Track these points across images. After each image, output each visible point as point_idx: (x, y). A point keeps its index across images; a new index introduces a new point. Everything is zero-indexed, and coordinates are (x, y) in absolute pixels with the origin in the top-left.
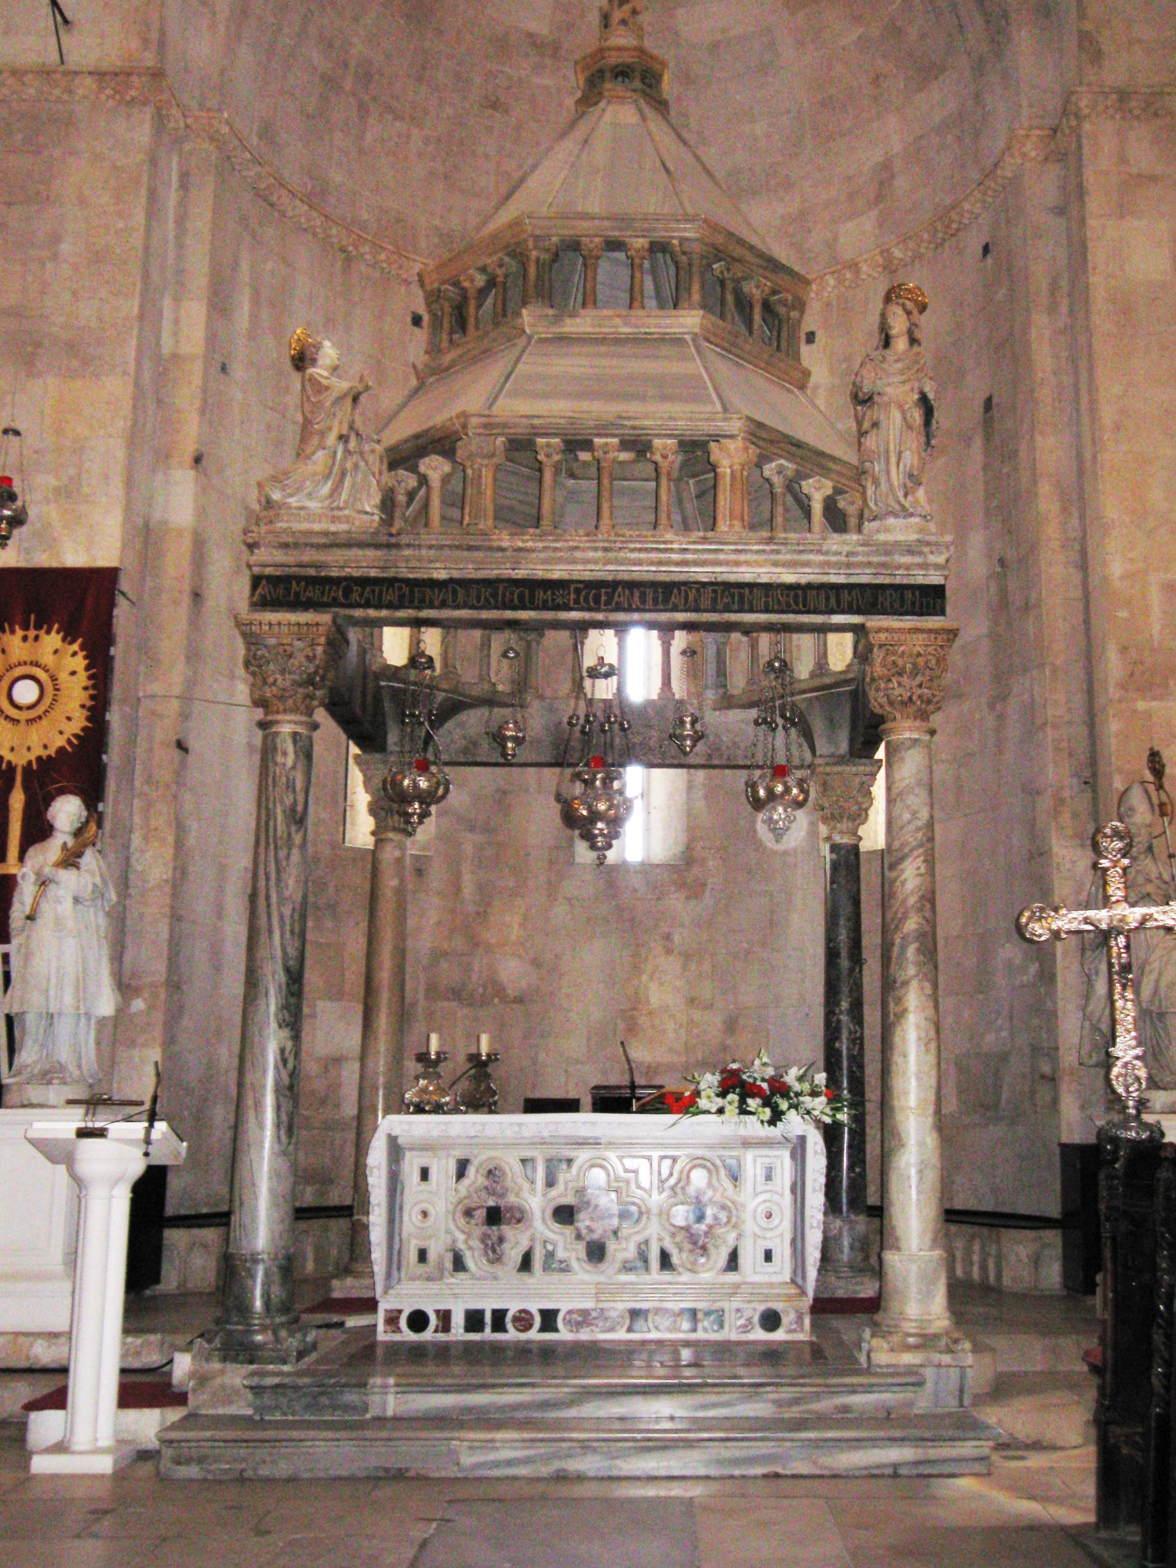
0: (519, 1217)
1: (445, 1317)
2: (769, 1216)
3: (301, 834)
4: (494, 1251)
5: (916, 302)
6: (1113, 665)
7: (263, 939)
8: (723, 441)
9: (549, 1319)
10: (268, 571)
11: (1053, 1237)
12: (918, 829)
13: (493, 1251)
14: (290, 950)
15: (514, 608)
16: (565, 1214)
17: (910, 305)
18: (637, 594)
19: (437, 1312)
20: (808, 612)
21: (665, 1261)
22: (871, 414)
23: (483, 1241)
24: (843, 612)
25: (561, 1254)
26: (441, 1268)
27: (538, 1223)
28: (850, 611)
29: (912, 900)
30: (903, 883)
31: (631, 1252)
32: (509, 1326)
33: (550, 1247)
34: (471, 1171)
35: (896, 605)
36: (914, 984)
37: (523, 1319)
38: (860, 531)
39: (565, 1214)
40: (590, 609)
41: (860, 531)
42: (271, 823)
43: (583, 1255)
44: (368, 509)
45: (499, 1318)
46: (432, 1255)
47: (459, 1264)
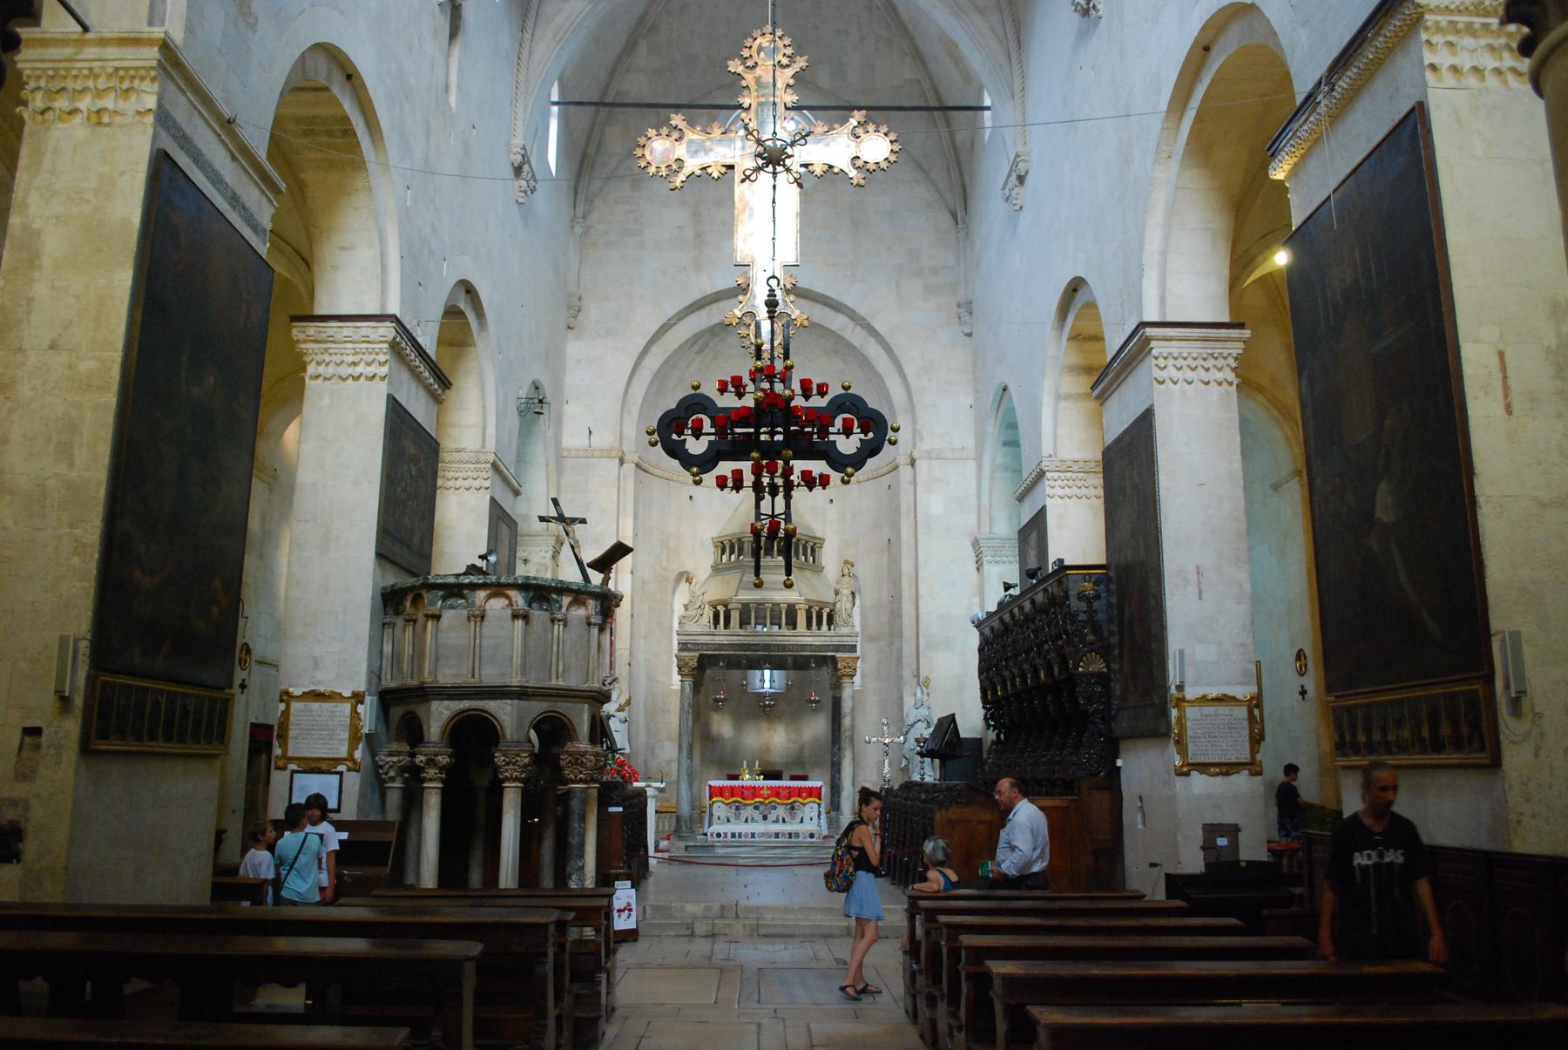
1: (726, 834)
9: (753, 835)
13: (737, 817)
17: (849, 566)
22: (839, 597)
26: (723, 820)
31: (775, 819)
36: (848, 749)
45: (740, 834)
46: (721, 818)
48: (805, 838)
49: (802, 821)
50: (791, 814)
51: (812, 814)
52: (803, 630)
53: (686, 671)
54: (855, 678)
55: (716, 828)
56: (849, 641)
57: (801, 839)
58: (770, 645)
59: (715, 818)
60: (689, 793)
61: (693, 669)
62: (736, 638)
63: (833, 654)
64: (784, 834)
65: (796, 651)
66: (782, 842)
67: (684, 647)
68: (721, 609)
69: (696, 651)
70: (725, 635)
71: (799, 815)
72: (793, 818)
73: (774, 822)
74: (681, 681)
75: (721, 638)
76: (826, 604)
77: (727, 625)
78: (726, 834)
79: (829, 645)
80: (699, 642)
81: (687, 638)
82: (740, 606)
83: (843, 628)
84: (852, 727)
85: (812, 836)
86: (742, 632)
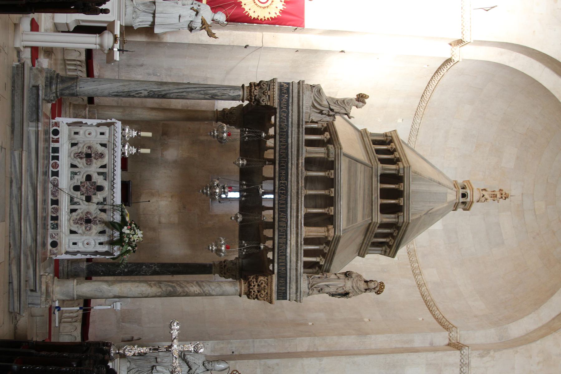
1: (57, 141)
2: (88, 244)
3: (208, 98)
4: (77, 156)
5: (378, 291)
7: (176, 87)
8: (333, 229)
9: (56, 174)
10: (291, 87)
12: (209, 291)
13: (78, 155)
14: (172, 95)
15: (279, 163)
16: (89, 178)
17: (377, 289)
18: (283, 202)
19: (58, 138)
20: (278, 256)
21: (73, 211)
22: (342, 276)
23: (80, 152)
24: (278, 267)
25: (76, 177)
26: (72, 139)
27: (86, 169)
28: (278, 270)
29: (186, 289)
30: (192, 286)
31: (76, 200)
32: (54, 161)
33: (78, 174)
34: (103, 148)
35: (280, 284)
36: (160, 290)
37: (56, 166)
38: (304, 273)
39: (89, 178)
40: (279, 187)
41: (304, 273)
42: (212, 89)
44: (311, 118)
45: (57, 158)
46: (76, 136)
47: (73, 145)
48: (52, 236)
49: (72, 232)
50: (81, 219)
51: (80, 245)
52: (303, 236)
53: (256, 92)
54: (245, 297)
57: (50, 231)
58: (286, 194)
59: (77, 129)
60: (106, 93)
61: (258, 101)
62: (295, 153)
63: (276, 271)
64: (57, 210)
65: (279, 226)
66: (44, 209)
67: (285, 89)
68: (327, 135)
69: (280, 103)
70: (298, 140)
71: (80, 229)
72: (76, 222)
74: (243, 86)
75: (295, 136)
76: (330, 261)
77: (310, 143)
78: (57, 141)
79: (286, 266)
80: (290, 108)
82: (332, 158)
83: (307, 282)
84: (187, 295)
85: (54, 244)
86: (302, 161)
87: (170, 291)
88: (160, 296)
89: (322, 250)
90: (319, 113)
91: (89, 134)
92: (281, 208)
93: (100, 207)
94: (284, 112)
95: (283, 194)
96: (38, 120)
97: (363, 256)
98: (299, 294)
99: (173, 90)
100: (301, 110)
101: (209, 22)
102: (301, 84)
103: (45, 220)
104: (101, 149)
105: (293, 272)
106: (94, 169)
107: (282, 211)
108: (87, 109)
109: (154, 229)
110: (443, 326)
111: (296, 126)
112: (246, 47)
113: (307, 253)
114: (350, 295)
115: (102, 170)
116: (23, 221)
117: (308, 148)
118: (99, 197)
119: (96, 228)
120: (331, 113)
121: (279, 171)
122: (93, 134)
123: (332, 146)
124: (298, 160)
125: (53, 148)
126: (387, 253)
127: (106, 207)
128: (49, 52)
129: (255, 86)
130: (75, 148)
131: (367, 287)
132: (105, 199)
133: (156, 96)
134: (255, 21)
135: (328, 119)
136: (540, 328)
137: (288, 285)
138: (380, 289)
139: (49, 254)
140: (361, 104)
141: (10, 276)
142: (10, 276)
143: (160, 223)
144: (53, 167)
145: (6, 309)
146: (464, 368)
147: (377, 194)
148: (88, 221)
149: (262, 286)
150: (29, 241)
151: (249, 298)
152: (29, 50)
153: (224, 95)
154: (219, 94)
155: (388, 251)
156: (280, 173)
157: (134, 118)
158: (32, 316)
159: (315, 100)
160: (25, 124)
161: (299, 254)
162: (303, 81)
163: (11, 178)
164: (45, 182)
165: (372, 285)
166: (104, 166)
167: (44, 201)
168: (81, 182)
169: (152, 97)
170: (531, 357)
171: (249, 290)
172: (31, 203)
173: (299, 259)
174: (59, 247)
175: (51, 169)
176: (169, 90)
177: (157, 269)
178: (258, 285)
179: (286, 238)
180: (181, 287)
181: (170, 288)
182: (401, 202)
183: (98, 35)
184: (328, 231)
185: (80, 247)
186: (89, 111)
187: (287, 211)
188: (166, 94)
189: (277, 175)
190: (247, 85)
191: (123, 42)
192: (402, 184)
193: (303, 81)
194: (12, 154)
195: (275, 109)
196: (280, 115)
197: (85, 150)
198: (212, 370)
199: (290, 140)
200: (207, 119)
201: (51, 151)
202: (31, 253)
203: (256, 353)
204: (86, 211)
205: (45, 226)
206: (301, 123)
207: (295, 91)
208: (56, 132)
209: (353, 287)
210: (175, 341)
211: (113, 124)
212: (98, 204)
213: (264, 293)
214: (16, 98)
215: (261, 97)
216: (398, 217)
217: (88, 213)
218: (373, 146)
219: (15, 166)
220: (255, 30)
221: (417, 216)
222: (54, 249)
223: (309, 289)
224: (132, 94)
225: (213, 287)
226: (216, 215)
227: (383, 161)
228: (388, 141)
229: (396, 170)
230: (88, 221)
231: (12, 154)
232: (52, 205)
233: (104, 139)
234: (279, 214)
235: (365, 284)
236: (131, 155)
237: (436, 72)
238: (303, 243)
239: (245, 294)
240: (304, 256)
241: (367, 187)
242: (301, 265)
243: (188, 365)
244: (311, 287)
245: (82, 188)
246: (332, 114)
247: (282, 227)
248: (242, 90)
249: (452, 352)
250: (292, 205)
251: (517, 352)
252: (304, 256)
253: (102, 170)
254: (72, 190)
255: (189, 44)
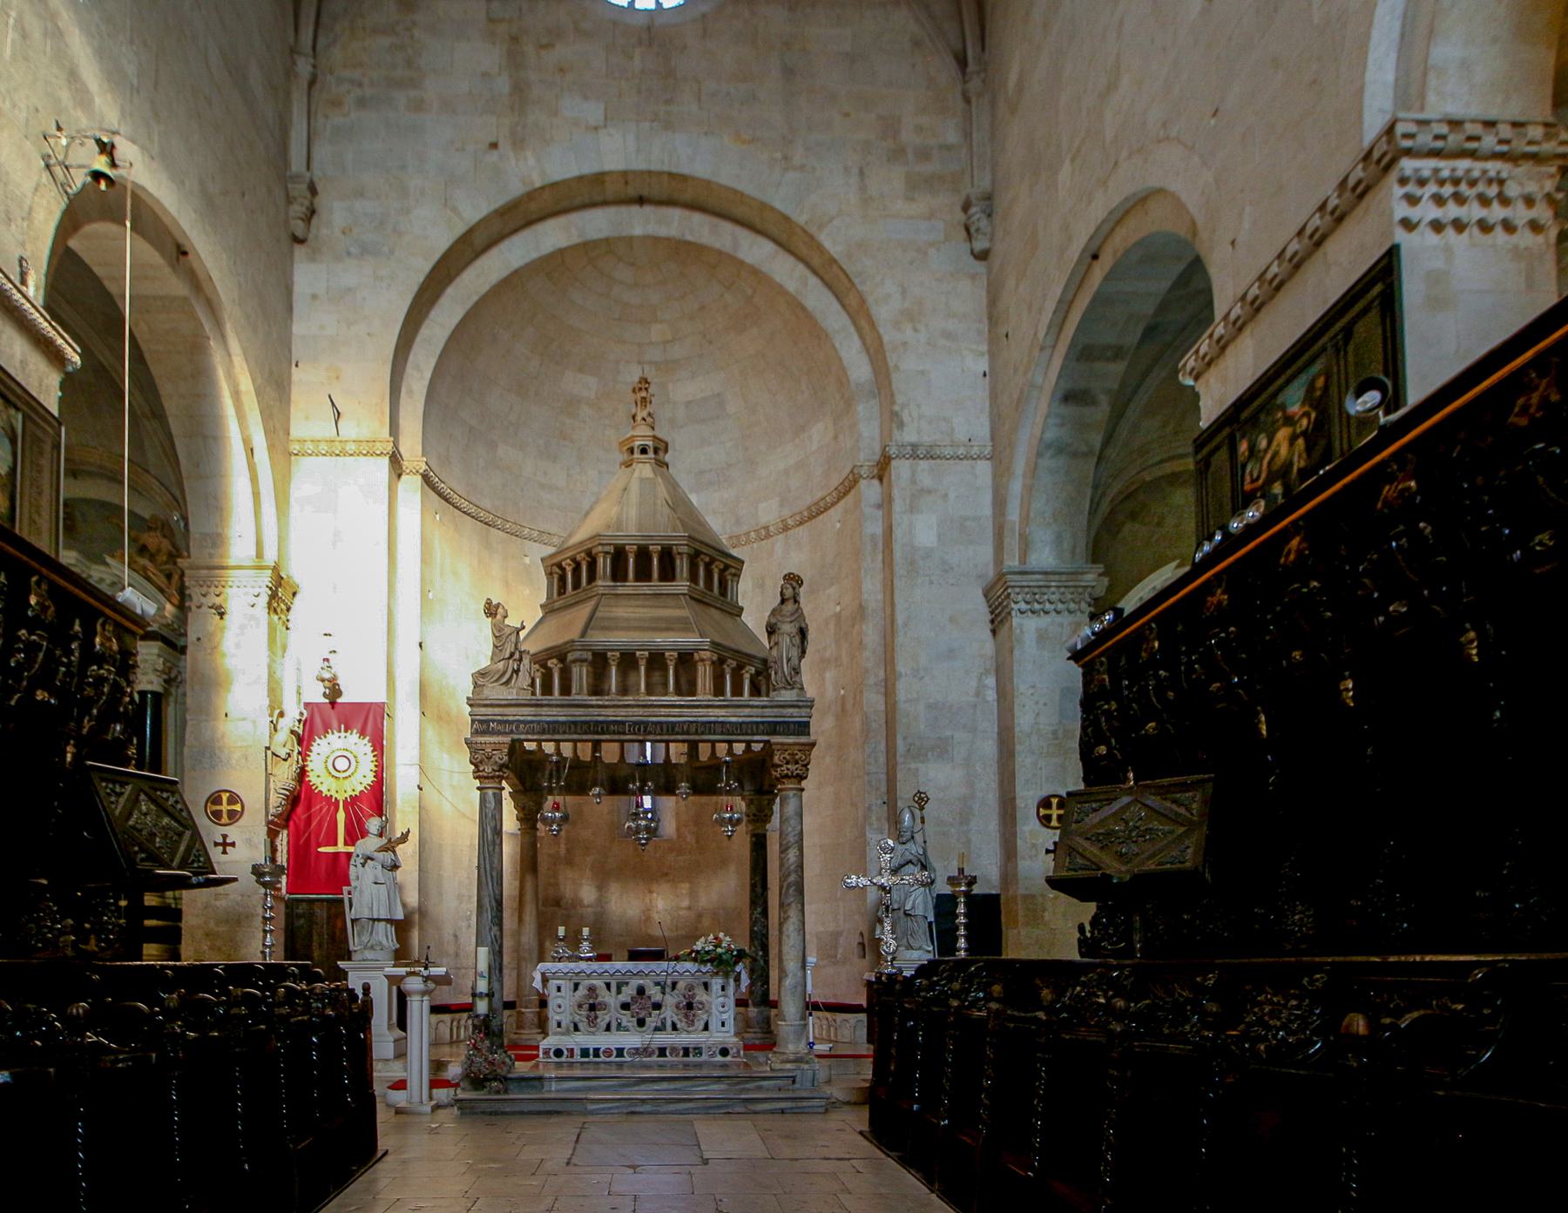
0: (604, 1006)
6: (901, 747)
7: (484, 886)
9: (620, 1052)
11: (863, 1017)
13: (592, 1021)
14: (497, 892)
16: (625, 1006)
17: (794, 584)
21: (674, 1027)
25: (624, 1024)
28: (763, 734)
29: (792, 867)
31: (659, 1024)
34: (581, 987)
36: (793, 905)
38: (768, 695)
39: (625, 1006)
40: (635, 734)
41: (768, 695)
43: (635, 1024)
45: (597, 1051)
46: (563, 1025)
47: (576, 1029)
48: (712, 1056)
49: (706, 1028)
50: (686, 1016)
51: (725, 1016)
54: (804, 783)
55: (550, 1042)
56: (794, 715)
57: (704, 1057)
58: (646, 723)
61: (502, 767)
63: (766, 738)
64: (674, 1050)
65: (696, 733)
66: (673, 1066)
67: (482, 726)
68: (551, 663)
69: (505, 734)
72: (692, 1023)
73: (657, 1029)
75: (555, 711)
77: (566, 690)
79: (757, 723)
80: (511, 718)
81: (490, 710)
83: (783, 692)
84: (801, 866)
85: (724, 1052)
86: (594, 700)
87: (795, 890)
88: (803, 905)
89: (733, 669)
90: (517, 675)
91: (560, 1007)
92: (668, 730)
93: (668, 990)
94: (517, 727)
95: (645, 728)
96: (540, 1079)
97: (742, 609)
98: (801, 704)
99: (489, 890)
100: (513, 702)
101: (384, 841)
102: (472, 702)
103: (688, 1065)
104: (582, 991)
105: (767, 711)
106: (611, 999)
107: (673, 729)
108: (523, 1010)
109: (700, 916)
110: (851, 488)
111: (539, 709)
112: (421, 789)
113: (737, 691)
114: (803, 625)
115: (614, 988)
116: (691, 1097)
117: (574, 691)
118: (654, 993)
119: (701, 996)
120: (517, 656)
121: (609, 734)
122: (559, 1001)
123: (569, 655)
124: (592, 706)
125: (582, 1057)
126: (738, 572)
127: (669, 982)
128: (438, 1065)
129: (479, 771)
130: (581, 1026)
131: (792, 601)
132: (657, 984)
133: (499, 914)
134: (379, 773)
135: (526, 661)
136: (859, 330)
137: (787, 719)
138: (793, 580)
139: (738, 1059)
140: (500, 610)
141: (772, 1112)
142: (772, 1112)
143: (689, 908)
144: (610, 1056)
145: (820, 1117)
146: (919, 452)
147: (644, 588)
148: (690, 1006)
149: (788, 757)
150: (722, 1087)
151: (806, 778)
152: (435, 1091)
153: (494, 817)
154: (493, 824)
155: (733, 571)
156: (614, 733)
157: (534, 944)
158: (829, 1082)
159: (496, 681)
160: (546, 1096)
161: (740, 703)
162: (468, 698)
163: (628, 1113)
164: (632, 1065)
165: (789, 592)
166: (608, 986)
167: (661, 1067)
168: (633, 1017)
169: (501, 919)
170: (905, 344)
171: (795, 777)
172: (665, 1085)
173: (746, 703)
174: (728, 1046)
175: (613, 1059)
176: (489, 896)
177: (759, 910)
178: (787, 763)
179: (714, 723)
180: (789, 875)
181: (791, 891)
182: (655, 549)
183: (408, 999)
184: (702, 660)
185: (729, 1016)
186: (526, 1007)
187: (672, 722)
188: (495, 899)
189: (616, 737)
190: (477, 783)
191: (418, 963)
192: (627, 547)
193: (468, 698)
194: (592, 1113)
195: (513, 741)
196: (523, 733)
197: (584, 1013)
198: (912, 832)
199: (560, 719)
200: (533, 845)
201: (586, 1060)
202: (738, 1083)
203: (885, 770)
204: (675, 1010)
205: (699, 1066)
206: (533, 702)
207: (483, 710)
208: (558, 1053)
209: (791, 622)
210: (875, 881)
211: (543, 974)
212: (664, 993)
213: (800, 755)
214: (508, 1110)
215: (496, 762)
216: (679, 554)
217: (677, 1007)
218: (567, 594)
219: (610, 1108)
220: (393, 776)
221: (678, 522)
222: (731, 1052)
223: (793, 688)
224: (497, 948)
225: (790, 829)
226: (678, 830)
227: (592, 577)
228: (558, 570)
229: (605, 558)
230: (690, 1006)
231: (592, 1113)
232: (666, 1056)
233: (567, 986)
234: (678, 734)
235: (786, 603)
236: (592, 949)
237: (447, 500)
238: (721, 698)
239: (800, 783)
240: (742, 695)
241: (633, 602)
242: (756, 701)
243: (904, 865)
244: (790, 684)
245: (641, 1016)
246: (517, 655)
247: (697, 730)
248: (484, 791)
249: (893, 472)
250: (662, 715)
251: (896, 366)
252: (742, 695)
253: (614, 988)
254: (644, 1029)
255: (420, 870)
